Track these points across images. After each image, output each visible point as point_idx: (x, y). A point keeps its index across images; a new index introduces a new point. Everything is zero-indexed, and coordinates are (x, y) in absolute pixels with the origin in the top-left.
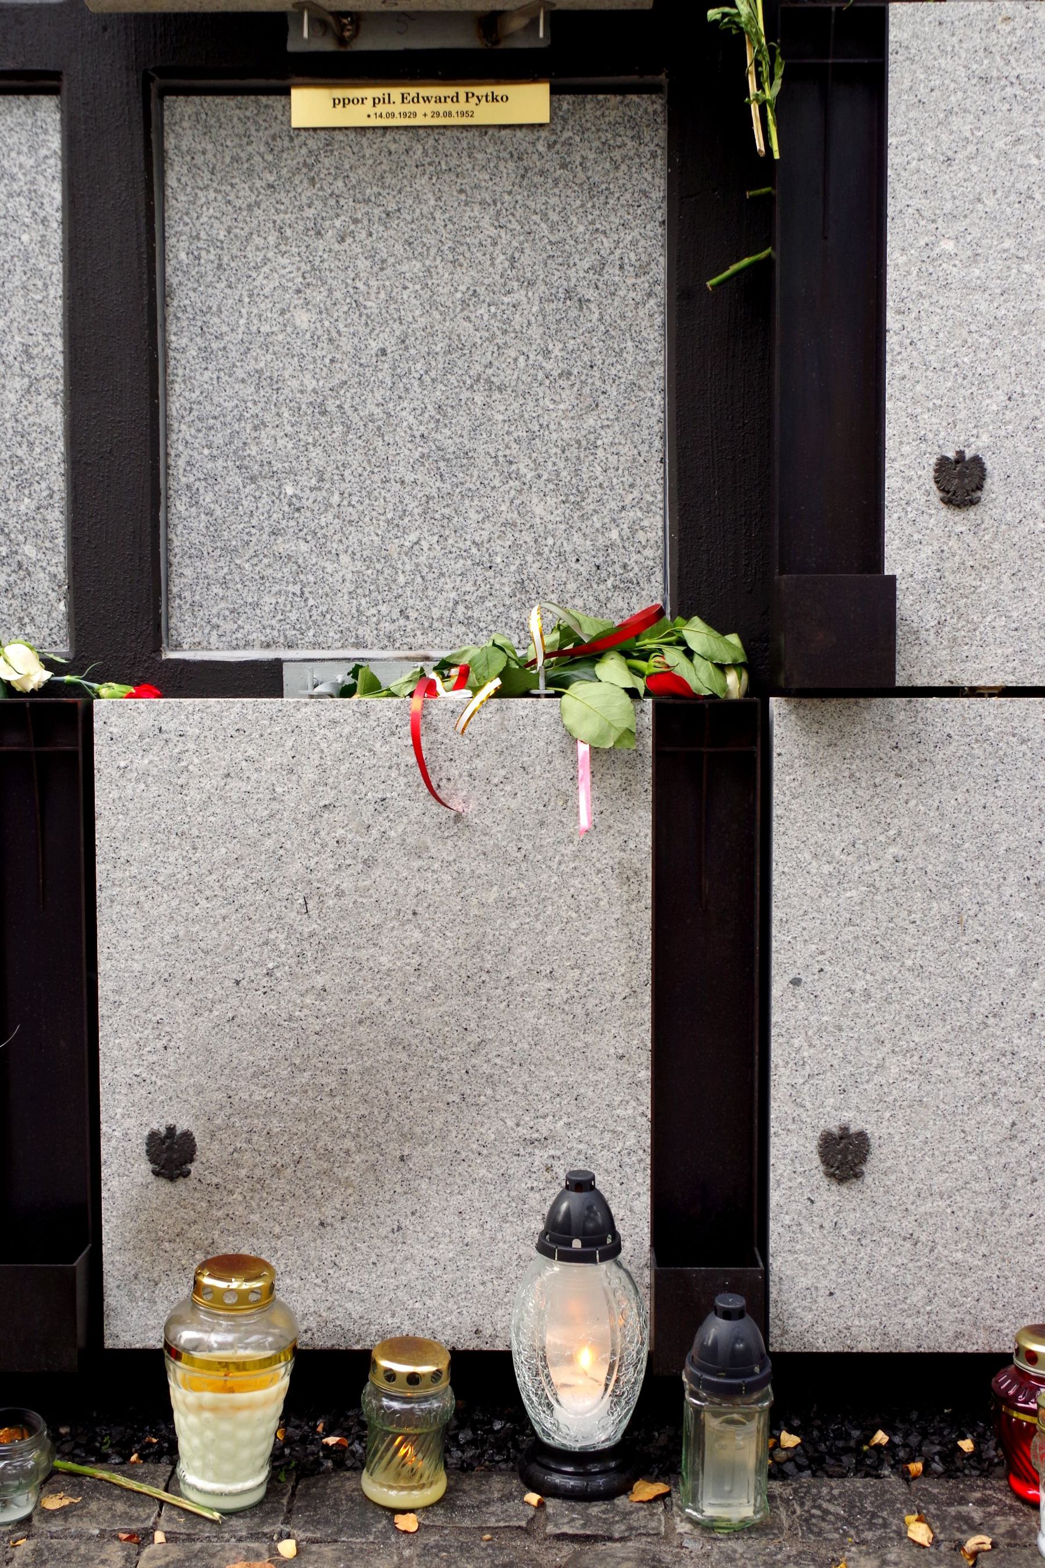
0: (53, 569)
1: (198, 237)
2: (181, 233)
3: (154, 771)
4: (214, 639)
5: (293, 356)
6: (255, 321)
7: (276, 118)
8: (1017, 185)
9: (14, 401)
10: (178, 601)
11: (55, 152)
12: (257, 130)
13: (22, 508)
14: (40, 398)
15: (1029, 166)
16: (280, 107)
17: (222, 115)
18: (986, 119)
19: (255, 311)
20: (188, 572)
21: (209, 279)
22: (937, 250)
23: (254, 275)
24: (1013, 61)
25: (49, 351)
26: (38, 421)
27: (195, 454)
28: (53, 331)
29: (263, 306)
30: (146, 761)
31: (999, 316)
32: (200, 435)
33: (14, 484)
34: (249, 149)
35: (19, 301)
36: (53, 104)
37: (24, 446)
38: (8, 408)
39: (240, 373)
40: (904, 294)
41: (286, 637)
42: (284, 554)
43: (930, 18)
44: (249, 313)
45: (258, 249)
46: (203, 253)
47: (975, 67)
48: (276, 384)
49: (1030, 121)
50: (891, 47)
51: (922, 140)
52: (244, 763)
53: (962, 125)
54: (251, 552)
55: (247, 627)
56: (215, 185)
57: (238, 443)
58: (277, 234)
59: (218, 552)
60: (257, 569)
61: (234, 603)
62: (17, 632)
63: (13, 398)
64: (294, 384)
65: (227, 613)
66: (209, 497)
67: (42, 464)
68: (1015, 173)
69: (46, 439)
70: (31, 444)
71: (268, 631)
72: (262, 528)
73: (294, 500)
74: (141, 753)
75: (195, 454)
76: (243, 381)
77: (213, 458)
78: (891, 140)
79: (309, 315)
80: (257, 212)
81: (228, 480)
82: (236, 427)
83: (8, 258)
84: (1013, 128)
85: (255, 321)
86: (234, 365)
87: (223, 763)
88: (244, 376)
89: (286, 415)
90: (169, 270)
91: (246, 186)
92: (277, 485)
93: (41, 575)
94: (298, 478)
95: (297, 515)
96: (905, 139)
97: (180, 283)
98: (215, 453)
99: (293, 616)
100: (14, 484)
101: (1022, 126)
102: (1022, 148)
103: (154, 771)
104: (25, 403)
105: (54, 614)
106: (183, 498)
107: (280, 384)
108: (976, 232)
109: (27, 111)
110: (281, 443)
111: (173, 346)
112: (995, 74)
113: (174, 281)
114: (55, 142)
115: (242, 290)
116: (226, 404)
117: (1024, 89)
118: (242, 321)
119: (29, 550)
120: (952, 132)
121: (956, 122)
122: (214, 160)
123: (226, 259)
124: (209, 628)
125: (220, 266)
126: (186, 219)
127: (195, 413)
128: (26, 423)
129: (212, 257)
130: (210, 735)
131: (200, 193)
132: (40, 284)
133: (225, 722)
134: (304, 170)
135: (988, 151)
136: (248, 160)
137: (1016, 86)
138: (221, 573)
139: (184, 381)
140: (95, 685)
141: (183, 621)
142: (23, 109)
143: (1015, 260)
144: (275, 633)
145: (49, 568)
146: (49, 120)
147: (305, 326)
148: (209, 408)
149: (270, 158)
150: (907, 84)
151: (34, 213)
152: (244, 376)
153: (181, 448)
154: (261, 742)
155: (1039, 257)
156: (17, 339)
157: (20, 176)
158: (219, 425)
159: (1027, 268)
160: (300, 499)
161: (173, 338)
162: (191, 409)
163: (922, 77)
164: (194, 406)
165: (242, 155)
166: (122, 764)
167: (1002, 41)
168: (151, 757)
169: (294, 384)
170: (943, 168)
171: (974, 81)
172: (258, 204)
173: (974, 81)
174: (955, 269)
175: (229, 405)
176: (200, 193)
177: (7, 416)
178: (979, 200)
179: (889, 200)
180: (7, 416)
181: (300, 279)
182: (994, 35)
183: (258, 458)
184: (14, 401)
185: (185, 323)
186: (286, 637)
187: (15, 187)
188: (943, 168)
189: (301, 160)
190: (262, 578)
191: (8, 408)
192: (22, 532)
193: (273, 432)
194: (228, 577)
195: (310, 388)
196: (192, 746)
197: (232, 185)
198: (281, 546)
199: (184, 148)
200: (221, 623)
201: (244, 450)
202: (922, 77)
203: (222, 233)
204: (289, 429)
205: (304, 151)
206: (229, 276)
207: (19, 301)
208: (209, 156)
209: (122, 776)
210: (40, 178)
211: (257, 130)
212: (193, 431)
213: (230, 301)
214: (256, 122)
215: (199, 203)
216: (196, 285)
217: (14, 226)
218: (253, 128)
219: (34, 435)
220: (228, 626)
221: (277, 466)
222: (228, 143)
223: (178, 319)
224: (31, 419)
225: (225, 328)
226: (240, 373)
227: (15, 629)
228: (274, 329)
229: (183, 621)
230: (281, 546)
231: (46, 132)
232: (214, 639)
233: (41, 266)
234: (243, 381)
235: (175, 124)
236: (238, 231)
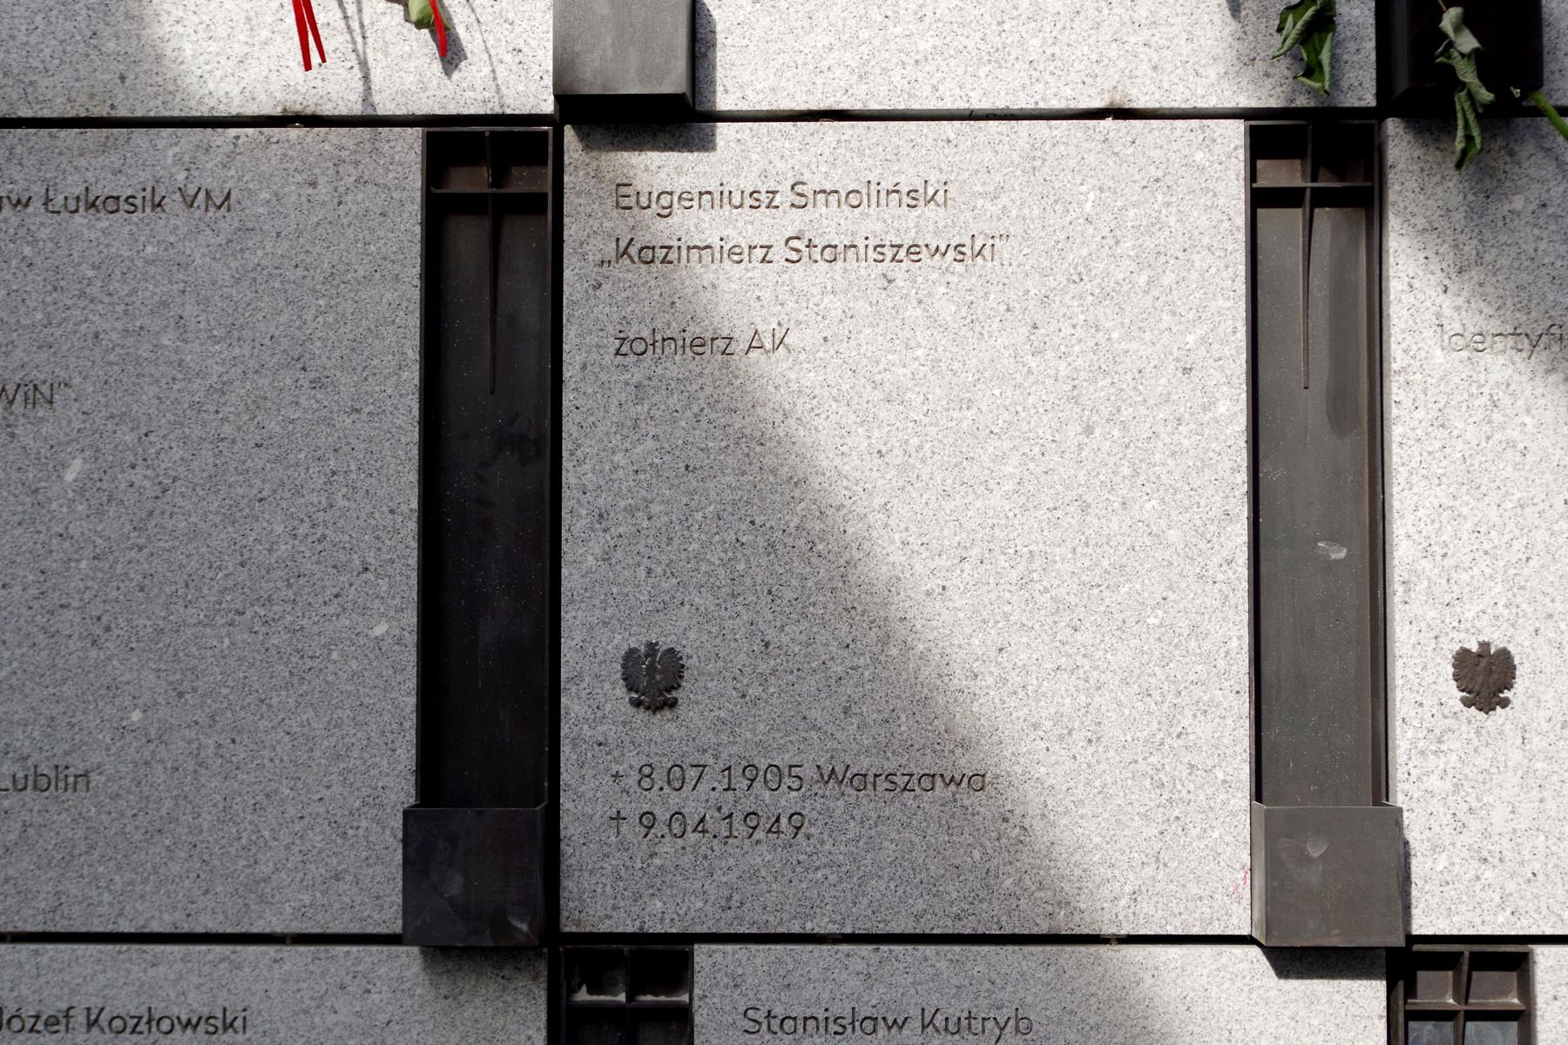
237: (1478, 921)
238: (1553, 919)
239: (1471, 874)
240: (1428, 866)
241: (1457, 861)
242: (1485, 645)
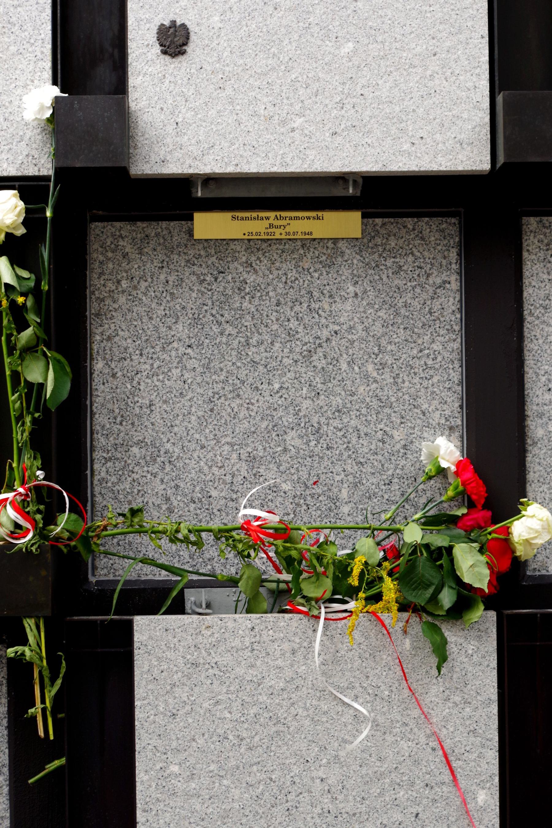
8: (218, 731)
15: (225, 718)
18: (196, 689)
22: (168, 772)
24: (213, 653)
31: (208, 812)
40: (148, 800)
43: (160, 627)
47: (189, 657)
49: (225, 691)
50: (136, 645)
51: (156, 703)
53: (182, 693)
68: (216, 723)
78: (137, 703)
84: (214, 695)
96: (145, 702)
101: (220, 693)
102: (220, 707)
108: (192, 760)
112: (202, 661)
117: (220, 671)
120: (175, 698)
121: (178, 691)
135: (199, 709)
137: (215, 669)
143: (218, 777)
150: (146, 668)
155: (232, 775)
159: (225, 782)
163: (156, 663)
167: (205, 641)
170: (170, 720)
171: (189, 666)
173: (189, 666)
174: (179, 784)
178: (194, 740)
179: (137, 741)
182: (200, 637)
188: (170, 720)
202: (156, 663)
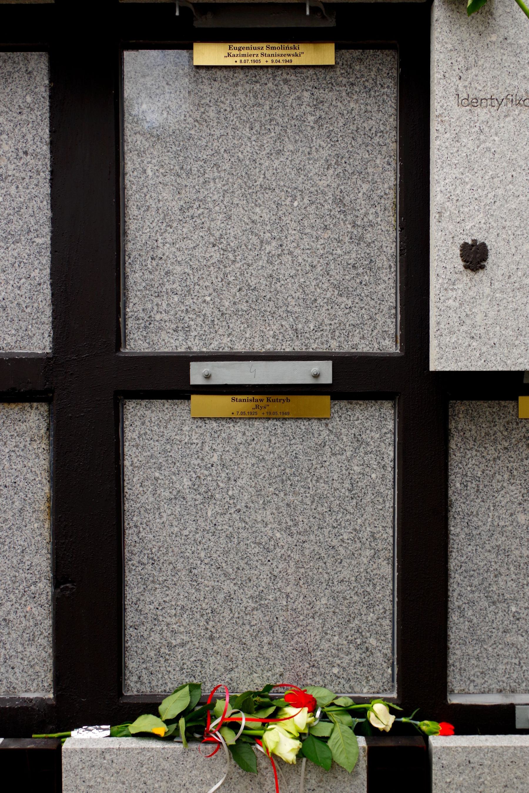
0: (385, 651)
1: (466, 475)
2: (457, 473)
3: (466, 784)
4: (471, 688)
5: (517, 538)
6: (496, 520)
7: (509, 413)
9: (366, 562)
10: (452, 667)
11: (391, 431)
12: (499, 419)
13: (369, 619)
14: (380, 560)
16: (511, 406)
17: (480, 411)
19: (497, 514)
20: (458, 652)
21: (472, 497)
23: (496, 495)
25: (385, 536)
26: (378, 572)
27: (463, 590)
28: (387, 525)
29: (501, 512)
30: (461, 779)
32: (466, 580)
33: (365, 606)
34: (495, 428)
35: (369, 509)
36: (390, 405)
37: (371, 586)
38: (363, 566)
39: (488, 547)
41: (510, 687)
42: (510, 643)
44: (493, 515)
45: (498, 481)
46: (469, 484)
48: (507, 553)
52: (515, 780)
54: (492, 642)
55: (490, 681)
56: (476, 448)
57: (486, 584)
58: (509, 473)
59: (475, 642)
60: (496, 650)
61: (483, 668)
62: (365, 684)
63: (365, 560)
64: (517, 553)
65: (479, 674)
66: (470, 613)
67: (380, 595)
69: (382, 582)
70: (374, 585)
71: (501, 683)
72: (498, 629)
73: (516, 614)
74: (458, 774)
75: (463, 590)
76: (489, 551)
77: (473, 592)
79: (525, 516)
80: (498, 462)
81: (481, 603)
82: (485, 575)
83: (364, 487)
85: (496, 520)
86: (485, 543)
87: (504, 780)
88: (490, 549)
89: (512, 569)
90: (450, 492)
91: (493, 448)
92: (506, 606)
93: (379, 654)
94: (518, 602)
95: (517, 622)
97: (456, 500)
98: (474, 589)
99: (515, 676)
100: (365, 606)
103: (466, 784)
104: (372, 563)
105: (385, 675)
106: (456, 613)
107: (509, 553)
109: (376, 409)
110: (509, 584)
111: (452, 532)
113: (453, 498)
114: (390, 425)
115: (489, 503)
116: (480, 563)
118: (490, 520)
119: (373, 641)
122: (476, 435)
123: (481, 487)
124: (469, 682)
125: (478, 490)
126: (460, 465)
127: (463, 568)
128: (372, 574)
129: (474, 486)
130: (497, 764)
131: (468, 452)
132: (381, 500)
133: (505, 758)
134: (524, 440)
136: (494, 435)
138: (476, 653)
139: (458, 551)
140: (418, 723)
141: (455, 678)
142: (373, 408)
144: (505, 685)
145: (383, 651)
146: (388, 413)
147: (523, 522)
148: (471, 565)
149: (506, 433)
151: (379, 463)
152: (490, 549)
153: (455, 587)
154: (525, 768)
156: (368, 529)
157: (371, 443)
158: (476, 574)
160: (519, 613)
161: (452, 528)
162: (461, 566)
164: (463, 565)
165: (491, 432)
166: (448, 780)
168: (464, 776)
169: (517, 553)
172: (499, 458)
175: (482, 564)
176: (468, 452)
177: (362, 570)
180: (362, 570)
181: (521, 498)
183: (497, 592)
184: (366, 562)
185: (459, 521)
186: (510, 687)
187: (369, 449)
189: (523, 435)
190: (498, 655)
191: (363, 566)
192: (369, 631)
193: (505, 578)
194: (480, 655)
195: (525, 555)
196: (486, 770)
197: (485, 448)
198: (509, 638)
199: (460, 428)
200: (476, 679)
201: (489, 588)
203: (480, 473)
204: (514, 577)
205: (524, 430)
206: (483, 496)
207: (369, 509)
208: (473, 432)
209: (448, 787)
210: (382, 444)
211: (499, 419)
212: (462, 578)
213: (483, 509)
214: (498, 415)
215: (467, 457)
216: (465, 501)
217: (367, 470)
218: (497, 418)
219: (376, 580)
220: (479, 681)
221: (507, 596)
222: (484, 426)
223: (455, 518)
224: (375, 572)
225: (480, 523)
226: (488, 547)
227: (364, 683)
228: (507, 524)
229: (455, 678)
230: (509, 638)
231: (386, 420)
232: (471, 688)
233: (382, 491)
234: (489, 551)
235: (455, 415)
236: (488, 472)
237: (469, 365)
238: (502, 364)
239: (467, 344)
240: (448, 339)
241: (461, 338)
242: (475, 241)
